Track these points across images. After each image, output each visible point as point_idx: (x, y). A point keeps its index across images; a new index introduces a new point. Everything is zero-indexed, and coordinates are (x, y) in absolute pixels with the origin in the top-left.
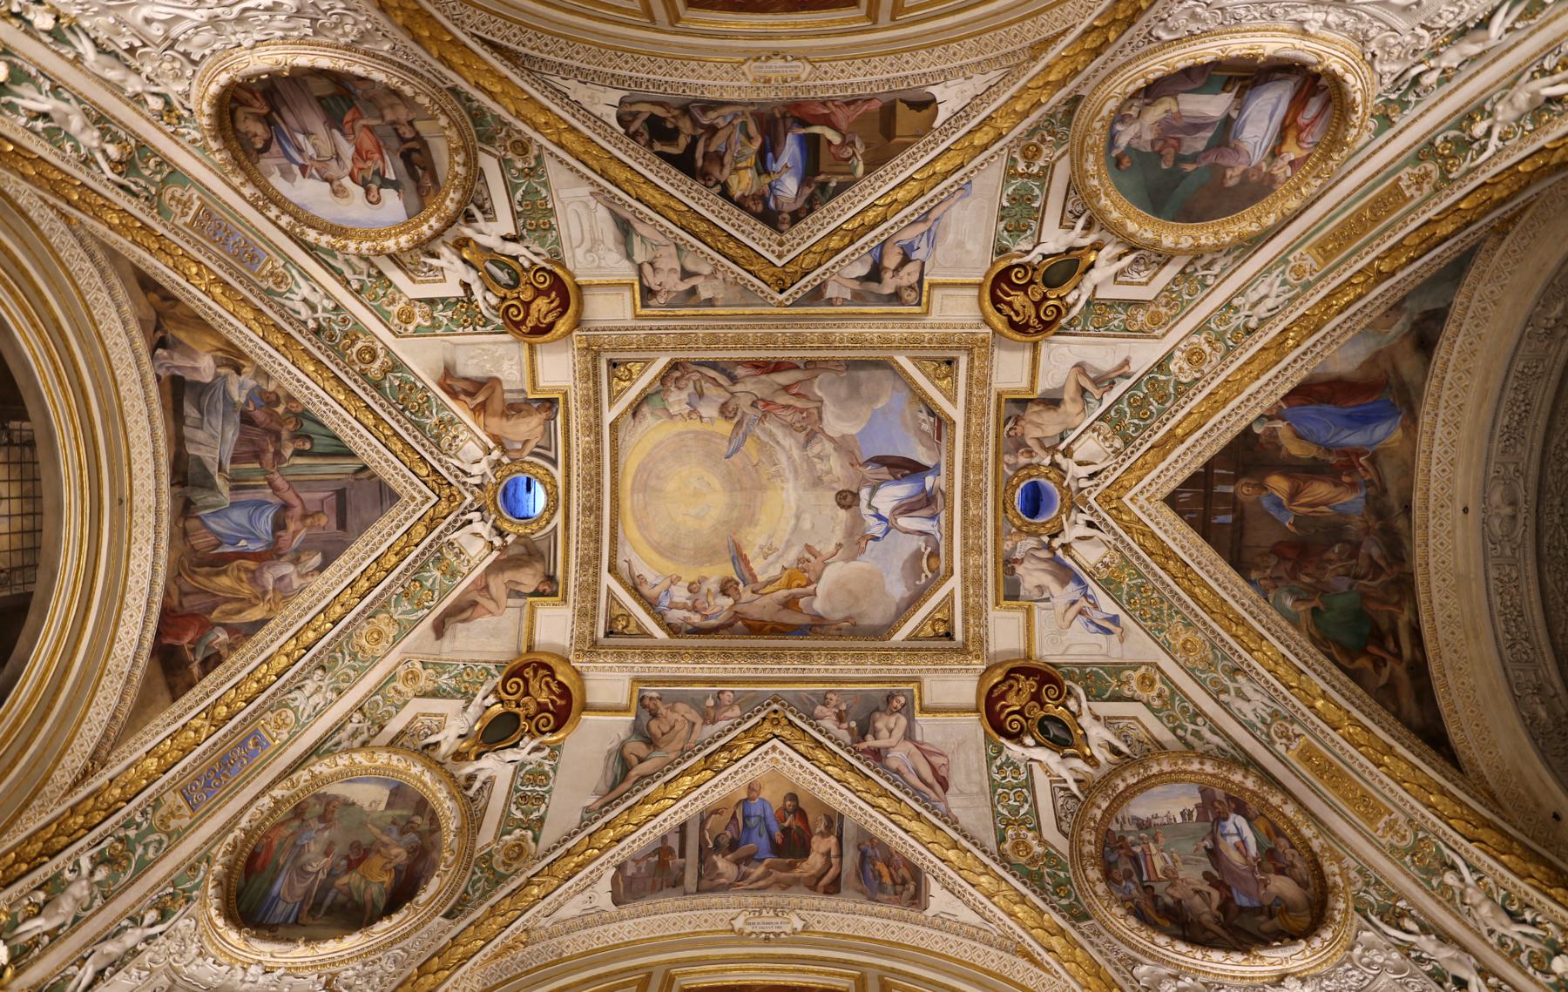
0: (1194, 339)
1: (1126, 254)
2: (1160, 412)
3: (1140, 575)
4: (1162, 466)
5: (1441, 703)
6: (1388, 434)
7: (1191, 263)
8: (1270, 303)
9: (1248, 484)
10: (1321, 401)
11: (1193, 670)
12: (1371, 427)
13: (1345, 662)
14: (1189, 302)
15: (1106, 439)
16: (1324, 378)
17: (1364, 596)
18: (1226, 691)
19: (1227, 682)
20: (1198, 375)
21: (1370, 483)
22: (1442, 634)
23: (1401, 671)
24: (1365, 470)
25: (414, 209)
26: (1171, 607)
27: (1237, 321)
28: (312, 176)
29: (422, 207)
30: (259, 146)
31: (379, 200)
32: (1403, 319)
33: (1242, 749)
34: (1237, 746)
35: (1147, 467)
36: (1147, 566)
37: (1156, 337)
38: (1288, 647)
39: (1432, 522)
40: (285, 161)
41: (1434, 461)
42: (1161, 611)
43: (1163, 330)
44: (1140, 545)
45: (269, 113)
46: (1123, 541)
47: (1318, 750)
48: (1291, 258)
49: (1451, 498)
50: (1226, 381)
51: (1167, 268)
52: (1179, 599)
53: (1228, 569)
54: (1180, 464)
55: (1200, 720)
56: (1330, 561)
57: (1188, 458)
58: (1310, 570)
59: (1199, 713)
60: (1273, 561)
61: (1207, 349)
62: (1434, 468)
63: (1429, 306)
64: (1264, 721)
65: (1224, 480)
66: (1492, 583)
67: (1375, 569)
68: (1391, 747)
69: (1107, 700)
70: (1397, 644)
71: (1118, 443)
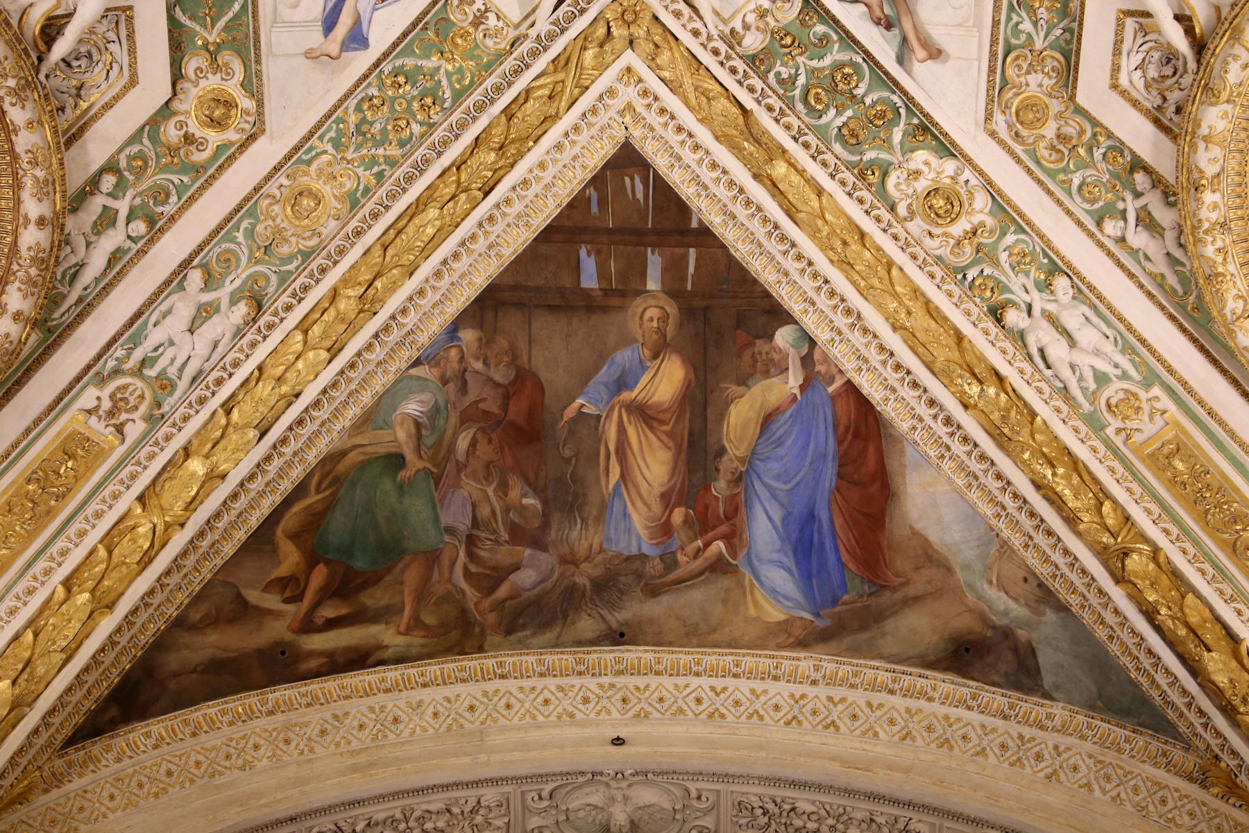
0: (981, 201)
1: (1189, 31)
2: (820, 132)
3: (459, 96)
4: (704, 135)
5: (211, 709)
6: (774, 593)
7: (1157, 181)
8: (1058, 350)
9: (664, 318)
10: (844, 461)
11: (251, 214)
12: (790, 562)
13: (290, 520)
14: (1066, 185)
15: (762, 14)
16: (892, 464)
17: (432, 558)
18: (210, 282)
19: (229, 288)
20: (902, 210)
21: (670, 562)
22: (358, 707)
23: (277, 630)
24: (698, 552)
26: (393, 163)
27: (1019, 286)
32: (1019, 611)
33: (81, 317)
34: (86, 308)
35: (701, 104)
36: (480, 108)
37: (989, 117)
38: (316, 404)
39: (591, 683)
41: (719, 683)
42: (382, 141)
43: (1004, 134)
44: (528, 92)
46: (535, 54)
47: (91, 469)
48: (1156, 391)
49: (642, 716)
50: (890, 265)
51: (1149, 128)
52: (410, 179)
53: (480, 281)
54: (707, 175)
55: (139, 227)
56: (503, 488)
57: (722, 192)
58: (484, 450)
59: (157, 228)
60: (501, 375)
61: (959, 228)
62: (705, 682)
63: (1045, 658)
64: (143, 363)
65: (673, 270)
66: (471, 794)
67: (490, 579)
68: (111, 607)
69: (171, 19)
70: (331, 624)
71: (753, 42)
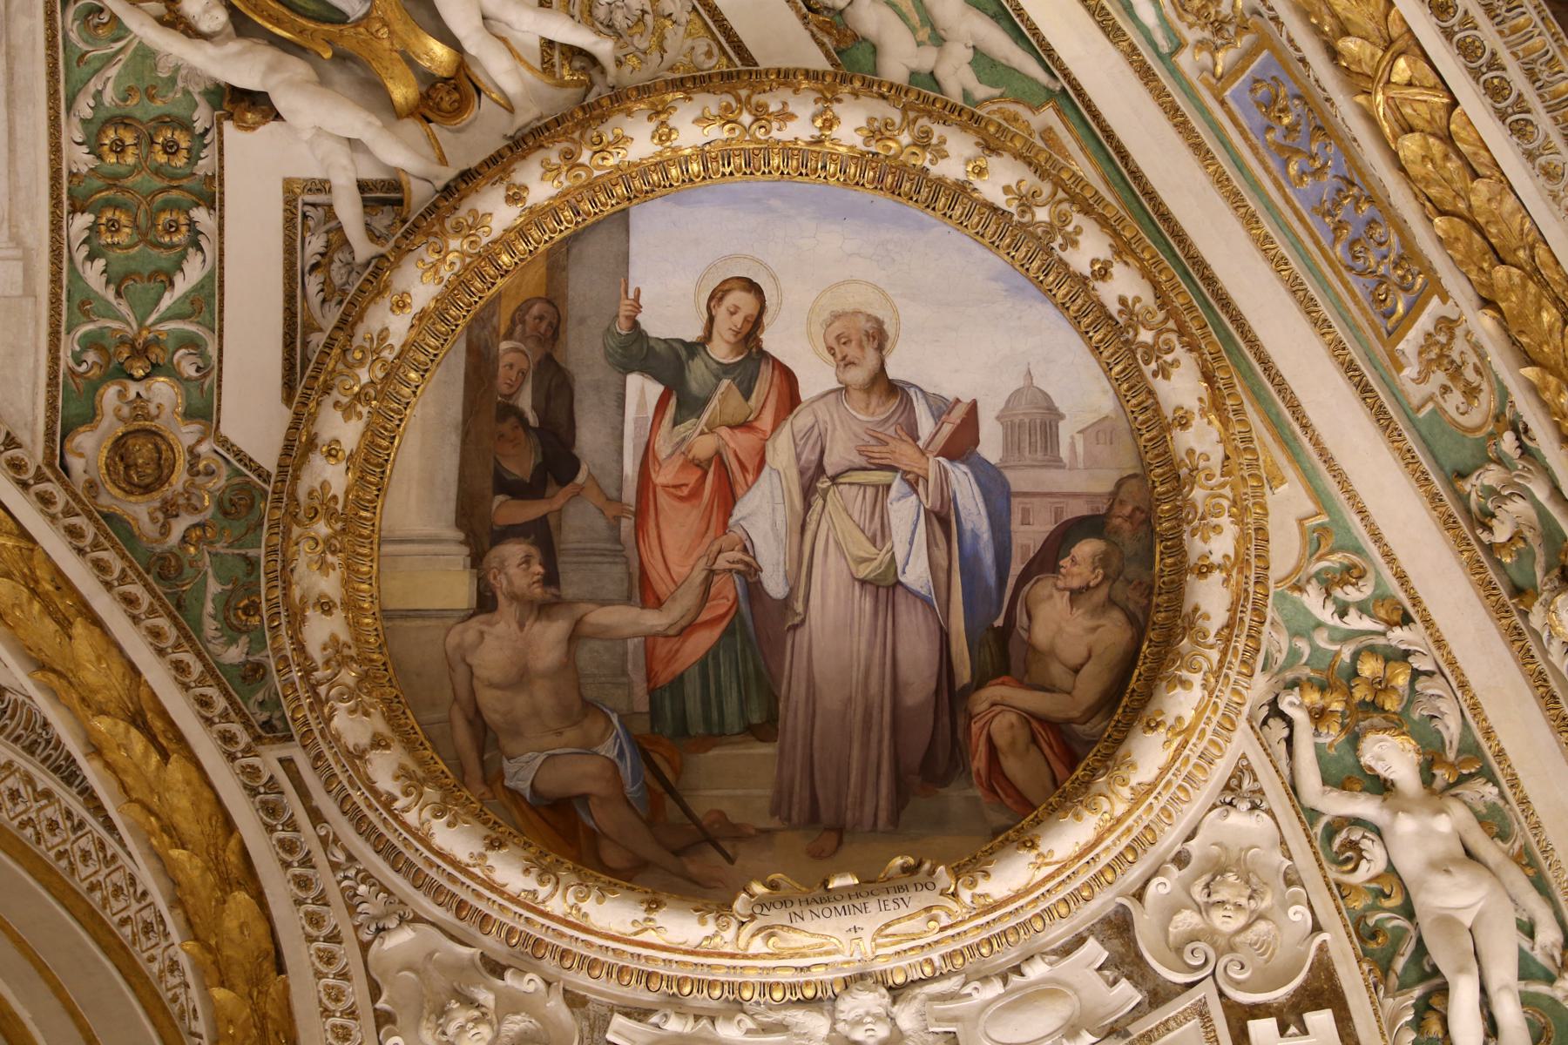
25: (594, 250)
28: (941, 408)
29: (558, 260)
30: (1086, 549)
31: (717, 296)
40: (1018, 480)
45: (979, 682)
